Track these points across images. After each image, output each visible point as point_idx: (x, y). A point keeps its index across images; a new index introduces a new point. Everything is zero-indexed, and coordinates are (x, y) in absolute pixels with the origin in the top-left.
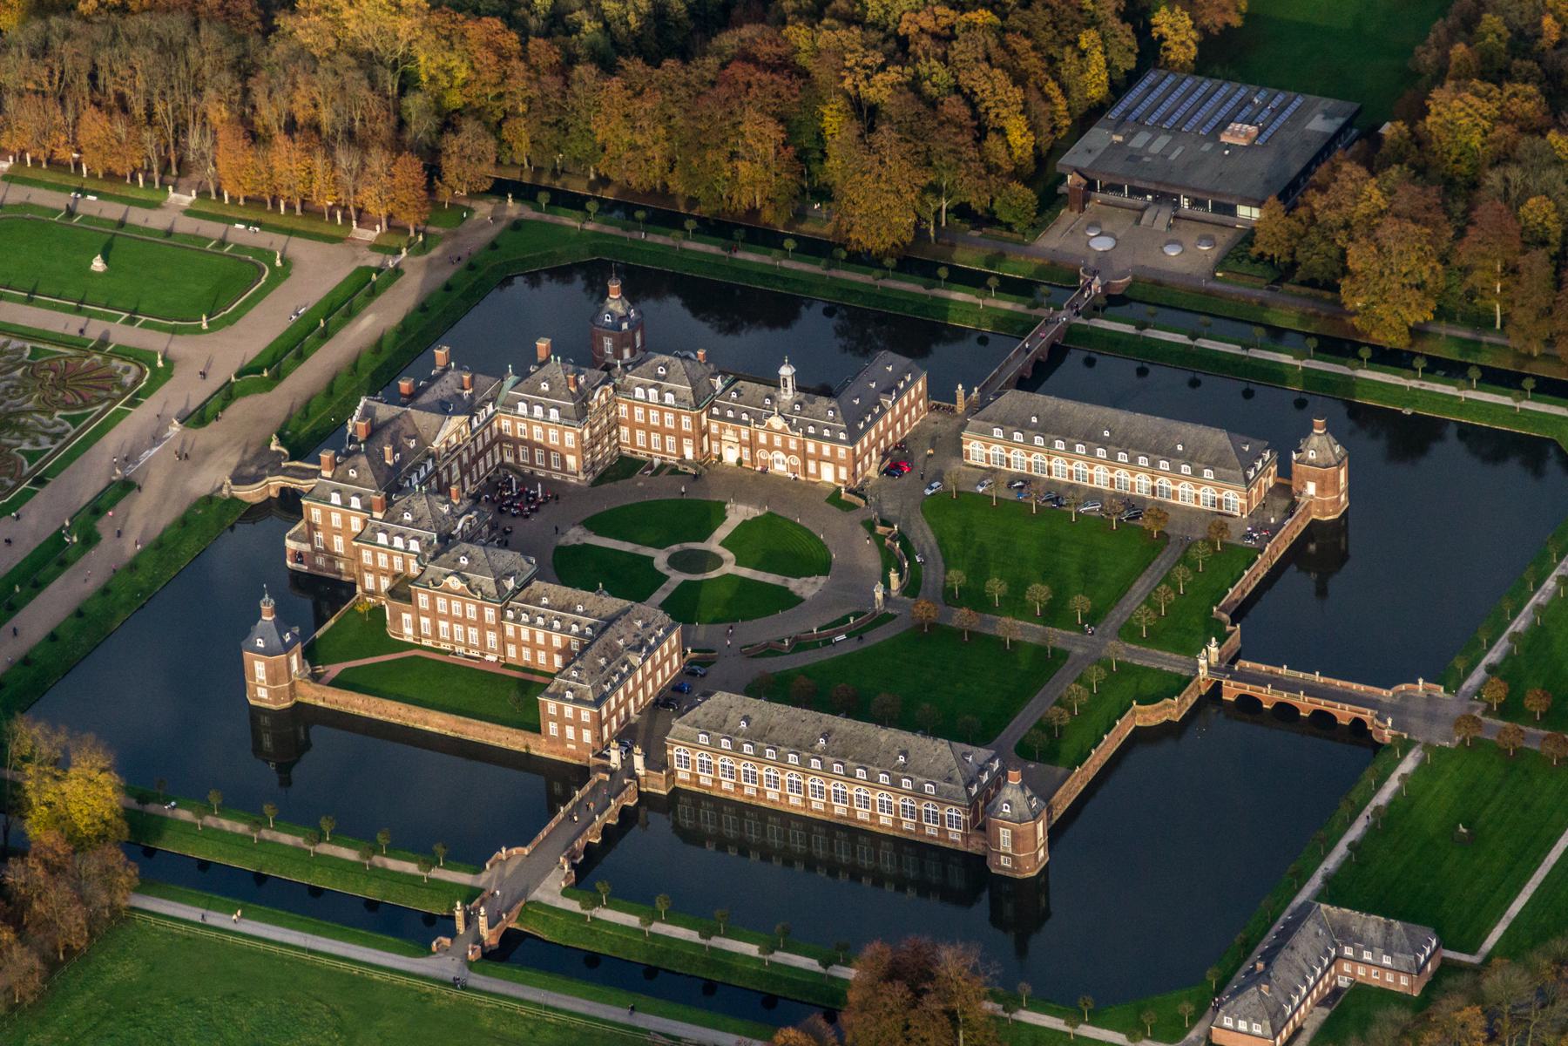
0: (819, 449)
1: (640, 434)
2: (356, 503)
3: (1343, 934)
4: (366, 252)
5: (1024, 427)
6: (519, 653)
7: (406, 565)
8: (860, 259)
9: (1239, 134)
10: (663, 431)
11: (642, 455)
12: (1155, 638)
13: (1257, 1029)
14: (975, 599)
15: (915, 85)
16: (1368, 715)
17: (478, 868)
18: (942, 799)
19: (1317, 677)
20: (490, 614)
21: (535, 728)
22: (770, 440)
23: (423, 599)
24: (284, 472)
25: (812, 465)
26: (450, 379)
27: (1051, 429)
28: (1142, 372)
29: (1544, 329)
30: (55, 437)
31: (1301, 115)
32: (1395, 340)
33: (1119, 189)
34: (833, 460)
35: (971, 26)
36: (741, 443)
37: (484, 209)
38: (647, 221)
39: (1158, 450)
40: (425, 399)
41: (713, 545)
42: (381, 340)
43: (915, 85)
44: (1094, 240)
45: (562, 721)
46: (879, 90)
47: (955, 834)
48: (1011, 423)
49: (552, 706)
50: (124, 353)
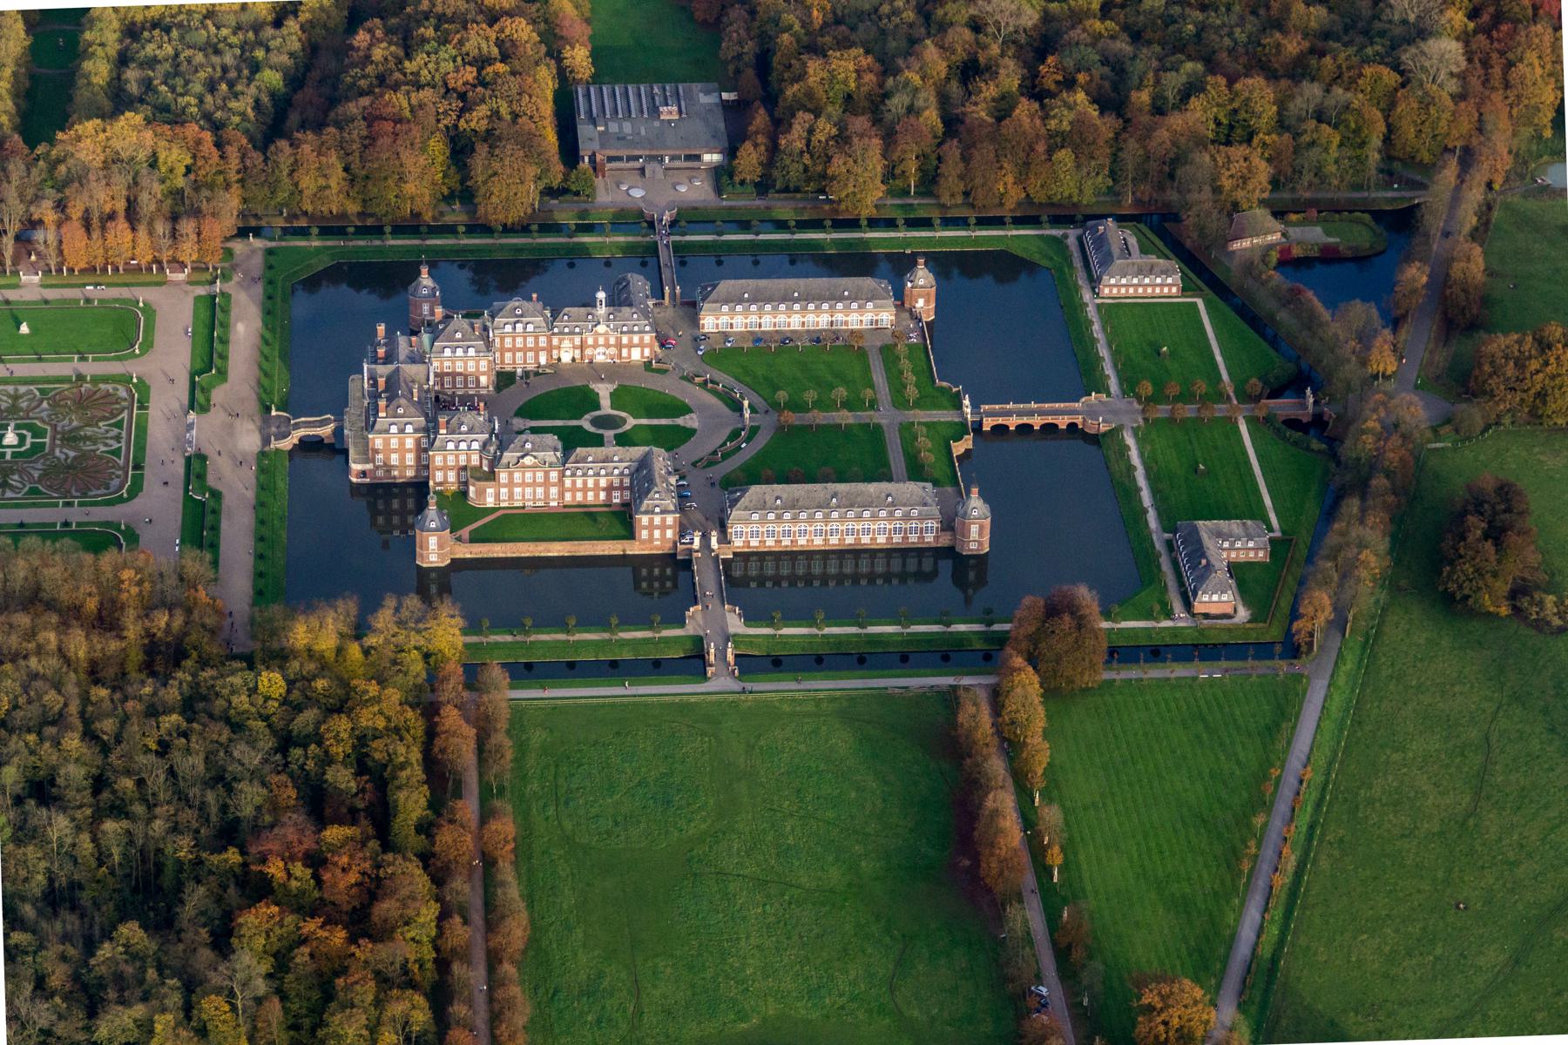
0: (631, 340)
1: (508, 355)
2: (409, 429)
3: (1219, 535)
4: (190, 288)
5: (740, 301)
6: (574, 497)
7: (469, 460)
8: (508, 230)
9: (669, 113)
10: (525, 350)
11: (508, 368)
12: (918, 404)
13: (1225, 598)
14: (797, 406)
15: (495, 114)
16: (1079, 420)
17: (681, 623)
18: (921, 518)
19: (1033, 405)
20: (554, 475)
21: (630, 533)
22: (596, 341)
23: (503, 477)
24: (297, 426)
25: (625, 352)
26: (402, 341)
27: (758, 298)
28: (720, 263)
29: (962, 187)
30: (118, 438)
31: (691, 98)
32: (866, 212)
33: (619, 159)
34: (642, 345)
35: (497, 74)
36: (574, 347)
37: (238, 246)
38: (355, 233)
39: (835, 298)
40: (402, 357)
41: (606, 407)
42: (262, 337)
43: (495, 114)
44: (619, 190)
45: (651, 527)
46: (477, 119)
47: (929, 538)
48: (734, 299)
49: (645, 520)
50: (96, 380)
